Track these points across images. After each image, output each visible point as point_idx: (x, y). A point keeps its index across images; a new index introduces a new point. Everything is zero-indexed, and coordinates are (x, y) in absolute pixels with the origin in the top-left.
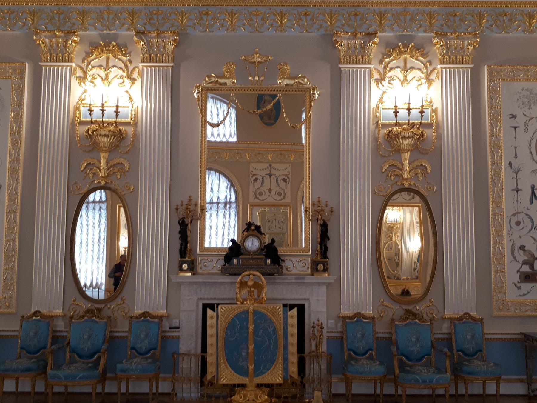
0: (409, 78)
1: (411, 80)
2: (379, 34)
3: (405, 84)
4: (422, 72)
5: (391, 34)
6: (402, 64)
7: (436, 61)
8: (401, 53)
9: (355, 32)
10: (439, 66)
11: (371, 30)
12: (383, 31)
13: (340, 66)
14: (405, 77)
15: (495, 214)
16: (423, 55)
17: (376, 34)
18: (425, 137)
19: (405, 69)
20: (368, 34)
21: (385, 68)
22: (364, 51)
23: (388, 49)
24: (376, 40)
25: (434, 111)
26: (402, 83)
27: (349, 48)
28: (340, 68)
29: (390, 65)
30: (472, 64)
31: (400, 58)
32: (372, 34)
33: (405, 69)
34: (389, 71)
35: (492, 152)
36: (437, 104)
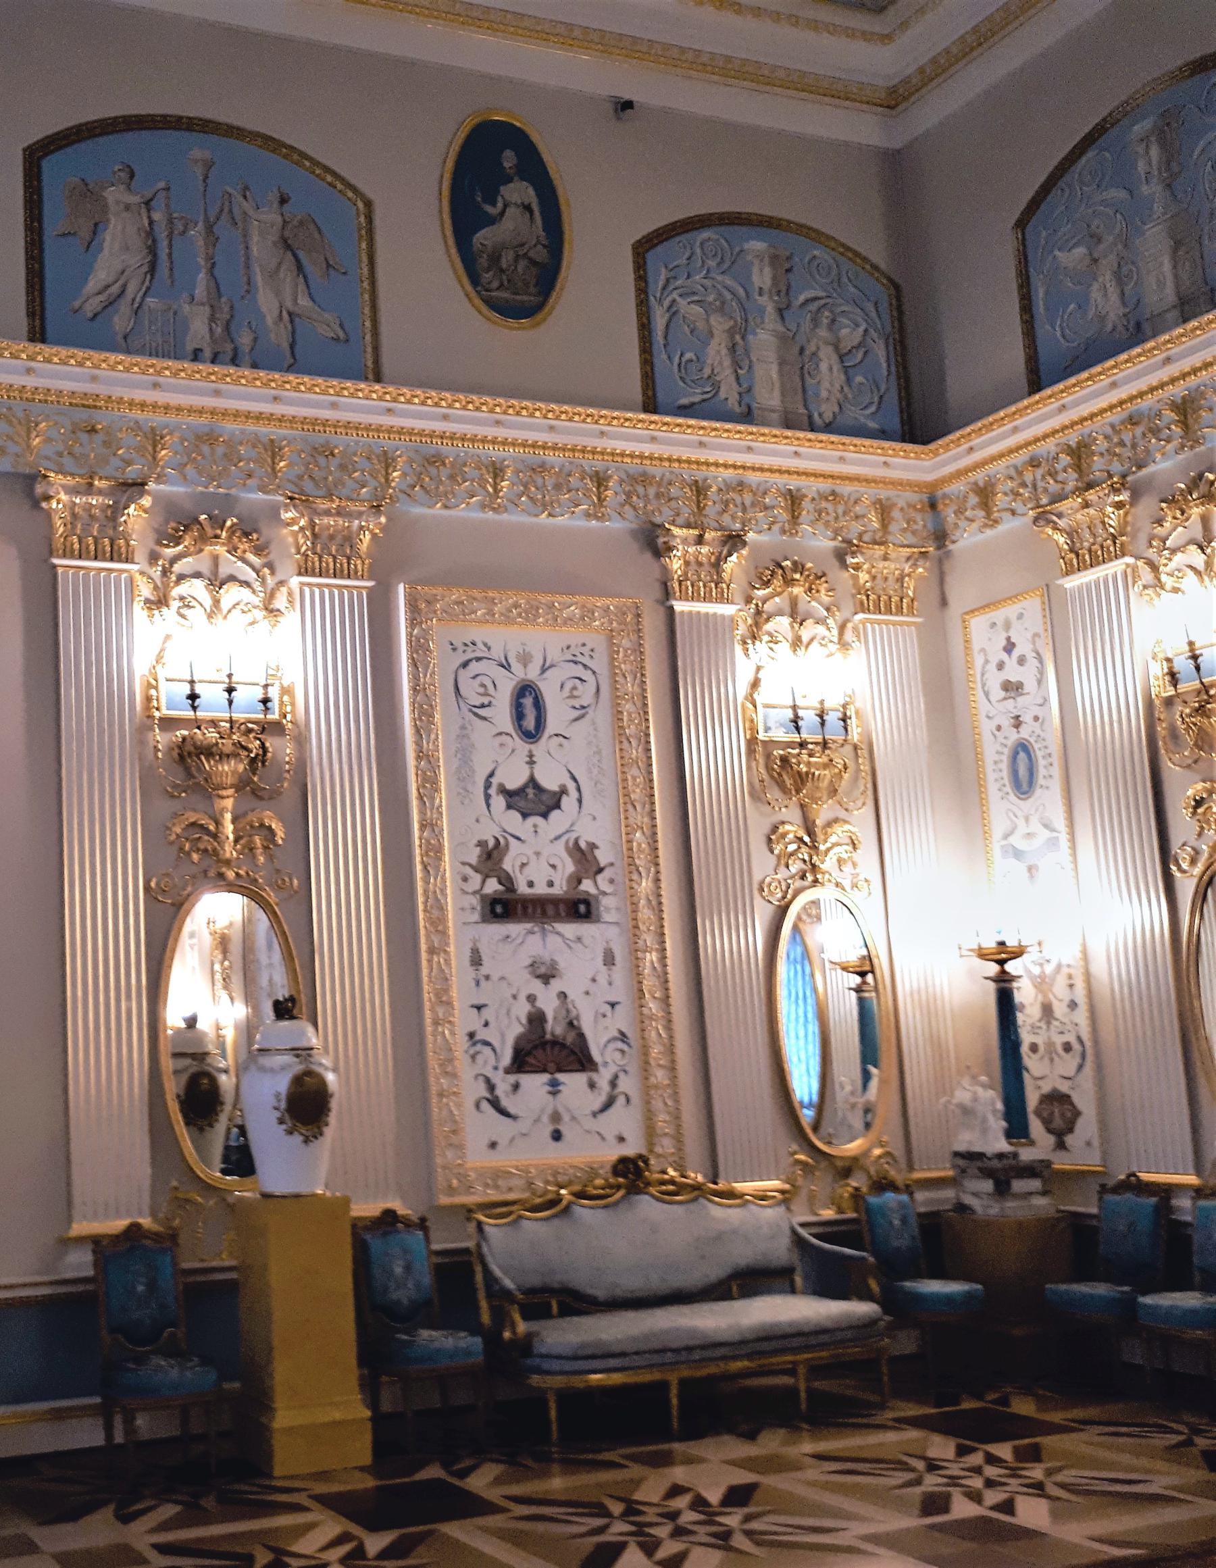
0: (225, 604)
1: (229, 611)
2: (151, 486)
3: (218, 619)
4: (254, 592)
5: (182, 489)
6: (205, 568)
7: (286, 569)
8: (203, 539)
9: (91, 477)
10: (295, 581)
11: (132, 472)
12: (159, 480)
13: (56, 561)
14: (216, 602)
15: (432, 951)
16: (259, 550)
17: (143, 484)
18: (269, 755)
19: (217, 582)
20: (125, 484)
21: (165, 572)
22: (115, 528)
23: (173, 525)
24: (146, 501)
25: (286, 691)
26: (210, 616)
27: (74, 516)
28: (55, 567)
29: (178, 568)
30: (370, 579)
31: (201, 550)
32: (134, 484)
33: (217, 582)
34: (178, 582)
35: (420, 797)
36: (293, 675)
